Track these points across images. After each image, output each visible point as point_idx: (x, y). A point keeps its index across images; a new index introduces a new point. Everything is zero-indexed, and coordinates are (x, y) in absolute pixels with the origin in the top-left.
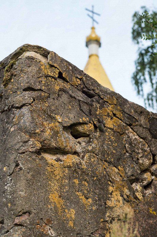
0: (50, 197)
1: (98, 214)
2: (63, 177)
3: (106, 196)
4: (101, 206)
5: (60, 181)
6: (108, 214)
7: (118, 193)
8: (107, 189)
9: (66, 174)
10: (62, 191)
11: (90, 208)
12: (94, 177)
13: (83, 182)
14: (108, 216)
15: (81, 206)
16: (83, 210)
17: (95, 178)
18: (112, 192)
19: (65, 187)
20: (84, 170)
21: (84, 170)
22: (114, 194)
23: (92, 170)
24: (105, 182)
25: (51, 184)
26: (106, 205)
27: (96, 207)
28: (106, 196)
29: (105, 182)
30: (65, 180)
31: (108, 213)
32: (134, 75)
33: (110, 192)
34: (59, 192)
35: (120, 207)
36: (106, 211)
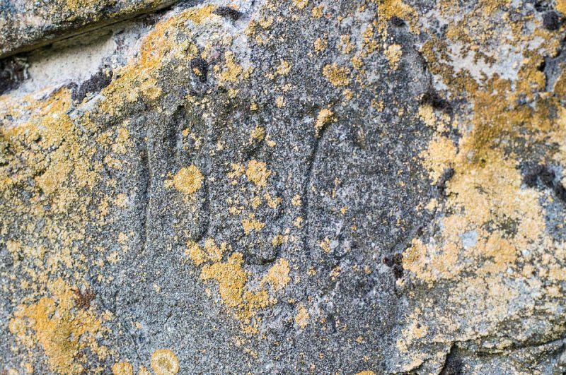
0: (13, 328)
1: (332, 346)
2: (100, 184)
3: (408, 212)
4: (362, 287)
5: (80, 213)
6: (412, 331)
7: (507, 173)
8: (413, 164)
9: (117, 164)
10: (100, 262)
11: (273, 325)
12: (314, 110)
13: (237, 167)
14: (416, 345)
15: (214, 325)
16: (226, 346)
17: (323, 114)
18: (450, 175)
19: (115, 241)
20: (232, 93)
21: (232, 93)
22: (462, 186)
23: (299, 71)
24: (395, 121)
25: (27, 250)
26: (399, 273)
27: (322, 307)
28: (408, 212)
29: (395, 121)
30: (114, 196)
31: (412, 327)
32: (48, 60)
33: (436, 176)
34: (77, 276)
35: (519, 266)
36: (394, 313)
